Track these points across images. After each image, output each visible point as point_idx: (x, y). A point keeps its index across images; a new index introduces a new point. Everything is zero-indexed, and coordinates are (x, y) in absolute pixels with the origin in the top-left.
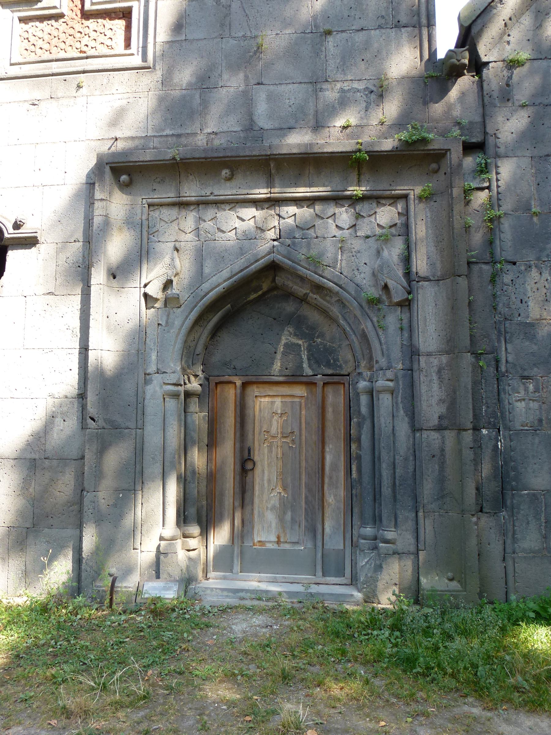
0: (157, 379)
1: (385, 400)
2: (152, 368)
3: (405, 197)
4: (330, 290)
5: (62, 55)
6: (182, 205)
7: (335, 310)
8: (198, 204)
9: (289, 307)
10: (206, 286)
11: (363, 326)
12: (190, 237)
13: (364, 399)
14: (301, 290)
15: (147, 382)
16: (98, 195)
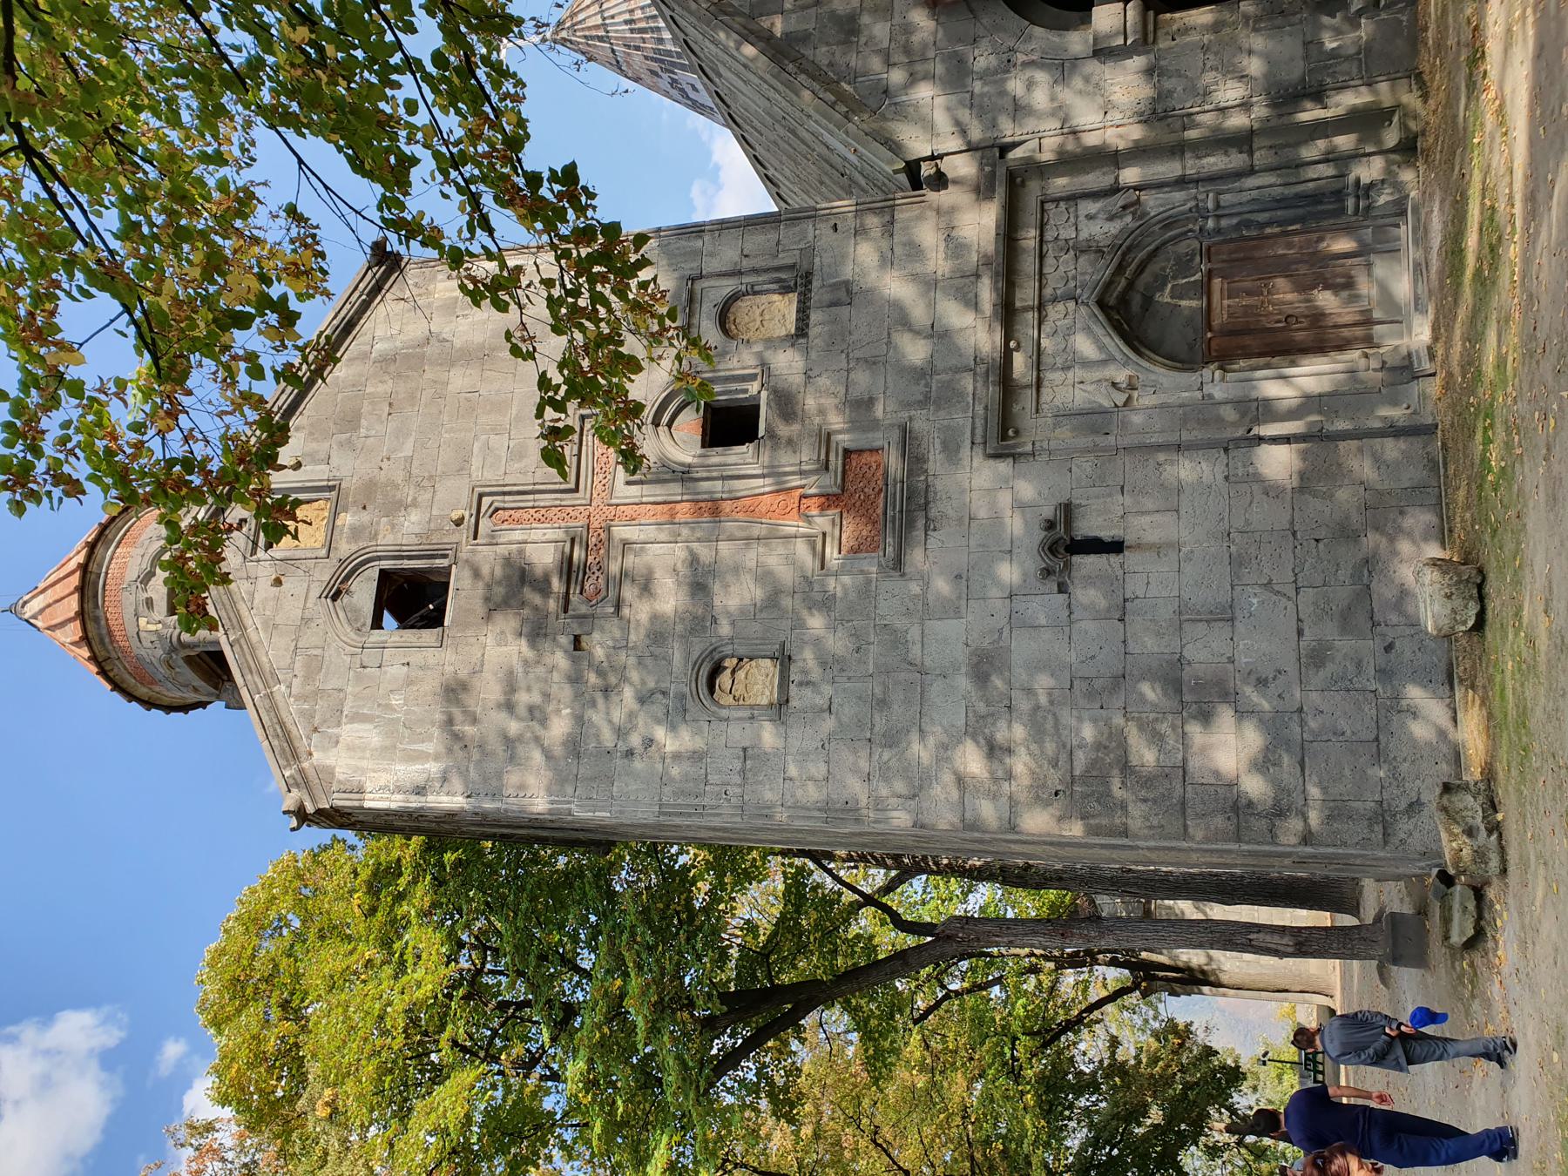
0: (1207, 389)
1: (1226, 199)
2: (1198, 395)
3: (1042, 203)
4: (1124, 255)
5: (880, 511)
6: (1039, 384)
7: (1142, 255)
8: (1039, 370)
9: (1136, 301)
10: (1118, 356)
11: (1156, 228)
12: (1070, 374)
13: (1224, 223)
14: (1123, 282)
15: (1210, 396)
16: (1029, 448)
